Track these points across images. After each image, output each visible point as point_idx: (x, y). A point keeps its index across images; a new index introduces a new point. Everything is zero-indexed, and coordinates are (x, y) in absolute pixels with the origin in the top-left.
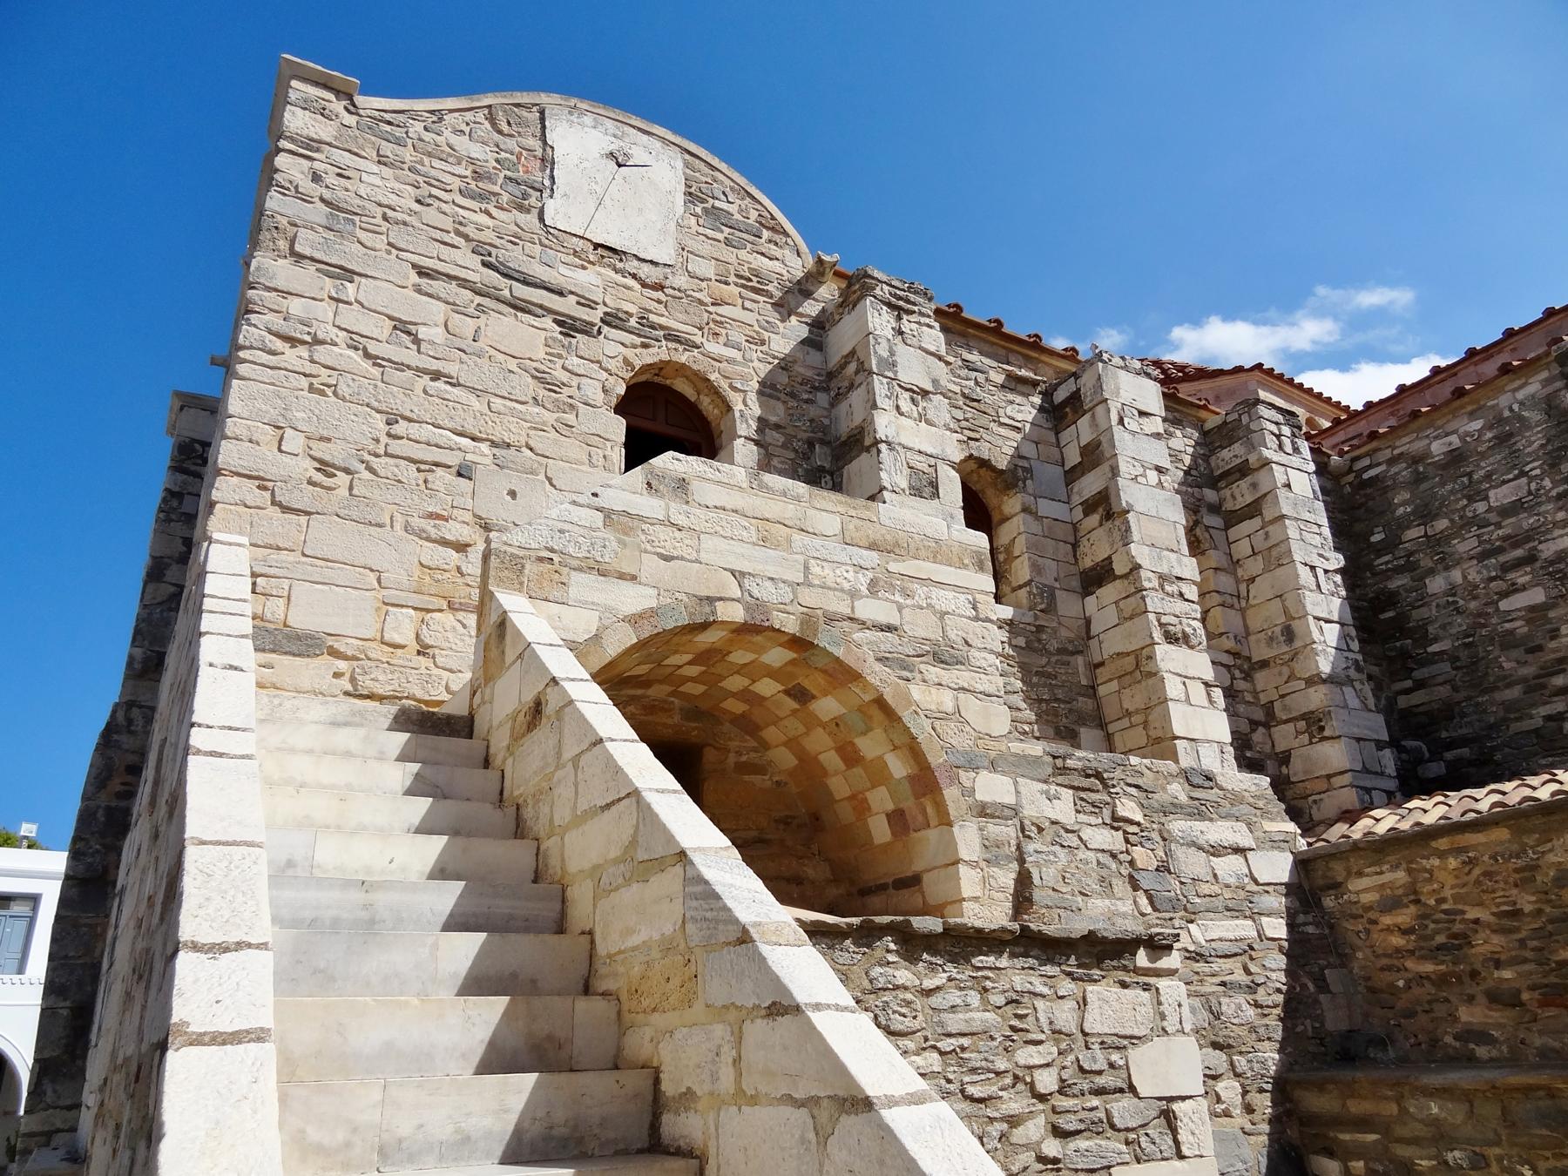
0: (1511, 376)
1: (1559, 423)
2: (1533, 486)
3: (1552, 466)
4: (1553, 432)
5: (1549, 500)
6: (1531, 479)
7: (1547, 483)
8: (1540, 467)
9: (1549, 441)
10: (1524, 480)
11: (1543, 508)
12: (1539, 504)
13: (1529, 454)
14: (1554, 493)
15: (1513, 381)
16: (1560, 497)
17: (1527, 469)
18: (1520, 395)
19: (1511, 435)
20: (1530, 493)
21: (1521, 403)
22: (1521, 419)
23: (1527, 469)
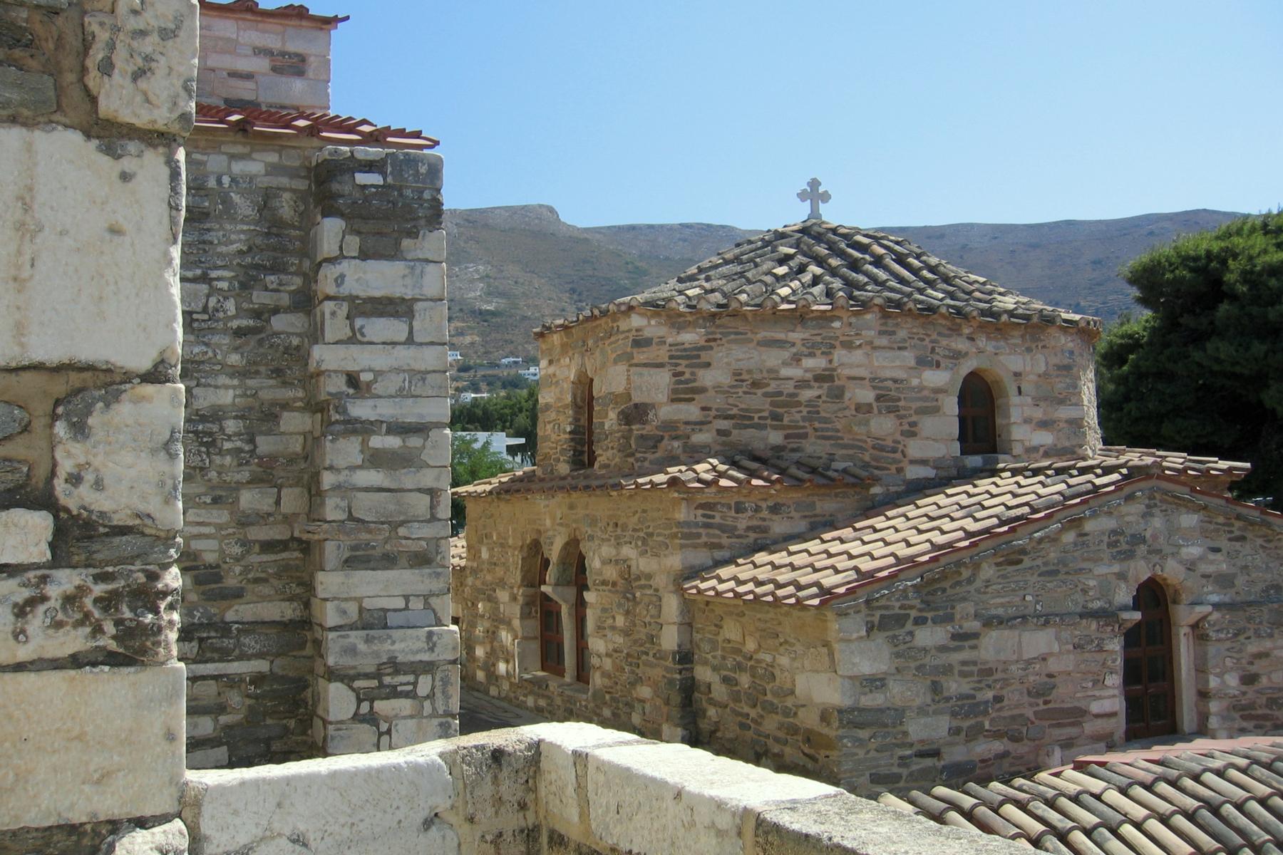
0: (239, 137)
1: (268, 234)
2: (212, 302)
3: (244, 286)
4: (258, 241)
5: (225, 331)
6: (213, 291)
7: (230, 306)
8: (230, 280)
9: (250, 249)
10: (204, 288)
11: (215, 339)
12: (212, 331)
13: (220, 255)
14: (235, 324)
15: (234, 143)
16: (239, 333)
17: (214, 274)
18: (237, 167)
19: (207, 215)
20: (205, 309)
21: (233, 180)
22: (226, 201)
23: (214, 274)
